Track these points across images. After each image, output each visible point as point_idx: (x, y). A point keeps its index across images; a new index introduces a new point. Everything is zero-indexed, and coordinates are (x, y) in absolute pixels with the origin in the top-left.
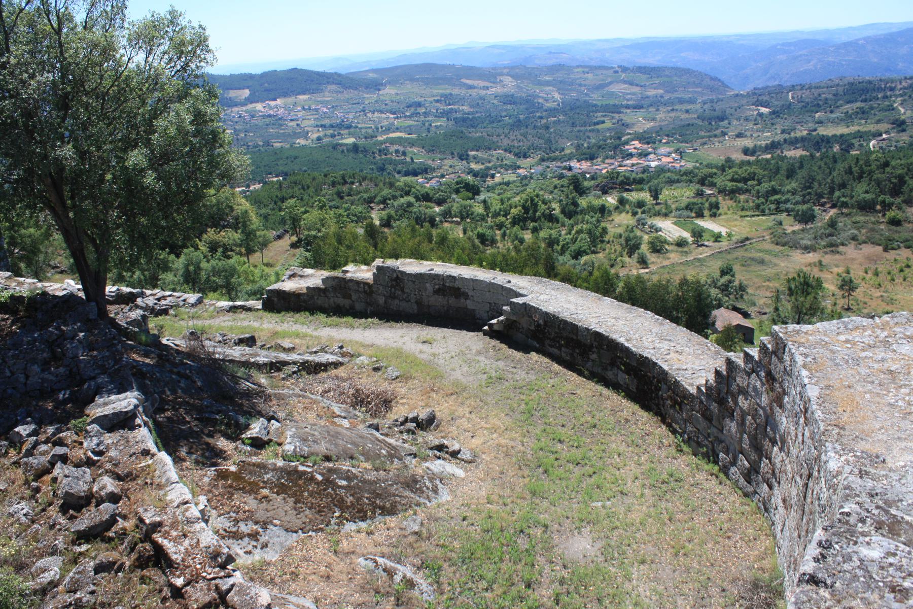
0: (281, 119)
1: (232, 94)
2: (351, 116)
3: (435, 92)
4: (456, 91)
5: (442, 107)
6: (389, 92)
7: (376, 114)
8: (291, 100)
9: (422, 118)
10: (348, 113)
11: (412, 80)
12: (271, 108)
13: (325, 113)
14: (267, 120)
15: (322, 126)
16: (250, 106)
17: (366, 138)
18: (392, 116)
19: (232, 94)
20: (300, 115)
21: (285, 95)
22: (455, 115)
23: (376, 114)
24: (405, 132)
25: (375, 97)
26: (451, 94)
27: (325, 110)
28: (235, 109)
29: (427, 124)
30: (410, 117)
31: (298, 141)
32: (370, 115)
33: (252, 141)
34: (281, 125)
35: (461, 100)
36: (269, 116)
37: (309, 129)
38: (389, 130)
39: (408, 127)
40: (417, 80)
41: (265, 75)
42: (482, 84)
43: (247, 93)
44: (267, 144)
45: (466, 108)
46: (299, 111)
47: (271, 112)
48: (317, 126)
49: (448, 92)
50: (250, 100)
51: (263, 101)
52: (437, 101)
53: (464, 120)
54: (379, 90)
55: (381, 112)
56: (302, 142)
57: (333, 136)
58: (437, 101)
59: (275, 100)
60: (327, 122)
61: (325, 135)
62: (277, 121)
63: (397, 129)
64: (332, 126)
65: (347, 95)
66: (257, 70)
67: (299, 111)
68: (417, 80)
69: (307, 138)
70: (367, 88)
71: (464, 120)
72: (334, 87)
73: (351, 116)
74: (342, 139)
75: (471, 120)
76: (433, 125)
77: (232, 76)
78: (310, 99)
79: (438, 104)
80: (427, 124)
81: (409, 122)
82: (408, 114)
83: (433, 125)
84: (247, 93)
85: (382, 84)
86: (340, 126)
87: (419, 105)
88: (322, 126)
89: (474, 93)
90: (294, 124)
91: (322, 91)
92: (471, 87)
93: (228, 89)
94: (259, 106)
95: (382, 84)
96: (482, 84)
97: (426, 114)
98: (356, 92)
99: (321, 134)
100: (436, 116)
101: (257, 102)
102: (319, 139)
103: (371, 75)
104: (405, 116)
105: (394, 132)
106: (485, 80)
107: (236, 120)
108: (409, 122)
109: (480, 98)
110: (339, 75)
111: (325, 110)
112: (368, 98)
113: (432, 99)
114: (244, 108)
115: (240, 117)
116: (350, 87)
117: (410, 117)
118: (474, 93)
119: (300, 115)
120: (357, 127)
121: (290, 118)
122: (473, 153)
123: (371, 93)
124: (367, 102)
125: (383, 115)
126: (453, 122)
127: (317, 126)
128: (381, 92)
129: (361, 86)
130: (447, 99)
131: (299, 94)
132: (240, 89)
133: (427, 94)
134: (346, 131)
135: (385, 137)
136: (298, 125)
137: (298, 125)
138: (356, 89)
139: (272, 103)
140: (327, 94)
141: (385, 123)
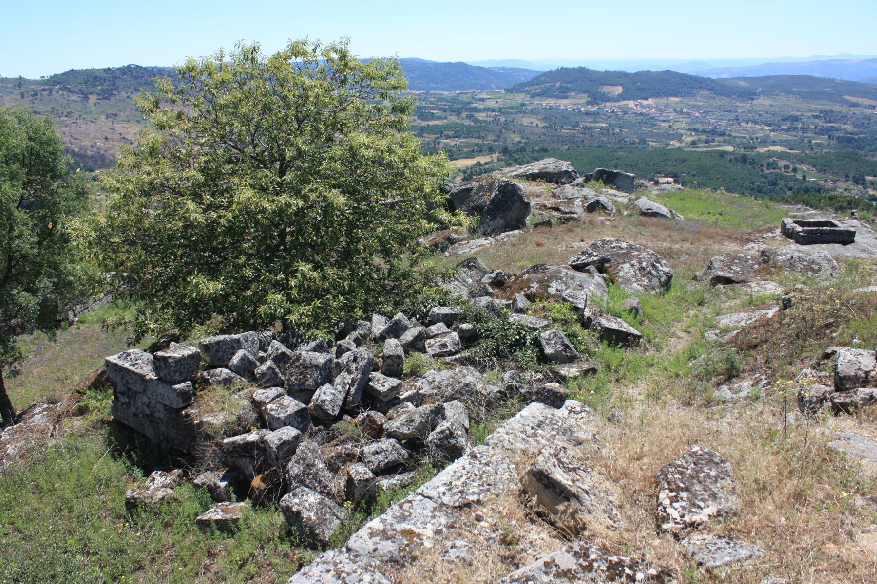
0: (653, 118)
1: (606, 89)
2: (724, 123)
3: (813, 106)
4: (837, 108)
5: (821, 123)
6: (763, 102)
7: (750, 124)
8: (662, 101)
9: (800, 133)
10: (720, 120)
11: (788, 92)
12: (642, 106)
13: (697, 117)
14: (640, 118)
15: (695, 130)
16: (623, 103)
17: (745, 148)
18: (767, 128)
19: (606, 89)
20: (672, 116)
21: (657, 95)
22: (837, 134)
23: (750, 124)
24: (785, 146)
25: (748, 106)
26: (832, 111)
27: (697, 114)
28: (608, 104)
29: (806, 140)
30: (787, 131)
31: (672, 142)
32: (743, 124)
33: (627, 137)
34: (654, 125)
35: (844, 118)
36: (642, 114)
37: (682, 132)
38: (764, 142)
39: (786, 141)
40: (794, 93)
41: (638, 74)
42: (868, 102)
43: (619, 90)
44: (644, 142)
45: (849, 127)
46: (671, 113)
47: (643, 111)
48: (690, 129)
49: (828, 108)
50: (622, 97)
51: (634, 98)
52: (816, 117)
53: (847, 140)
54: (753, 99)
55: (756, 123)
56: (677, 144)
57: (707, 142)
58: (816, 117)
59: (647, 99)
60: (698, 126)
61: (699, 140)
62: (650, 121)
63: (774, 143)
64: (704, 132)
65: (719, 101)
66: (631, 69)
67: (671, 113)
68: (794, 93)
69: (681, 141)
70: (740, 96)
71: (849, 140)
72: (705, 92)
73: (724, 123)
74: (718, 146)
75: (856, 141)
76: (813, 142)
77: (606, 72)
78: (681, 102)
79: (816, 121)
80: (806, 140)
81: (785, 137)
82: (784, 127)
83: (813, 142)
84: (619, 90)
85: (755, 94)
86: (714, 132)
87: (796, 119)
88: (695, 130)
89: (858, 111)
90: (666, 125)
91: (694, 95)
92: (854, 105)
93: (602, 84)
94: (631, 104)
95: (755, 94)
96: (868, 102)
97: (804, 130)
98: (728, 100)
99: (695, 138)
100: (815, 133)
101: (630, 99)
102: (693, 143)
103: (742, 83)
104: (782, 130)
105: (774, 145)
106: (870, 99)
107: (609, 115)
108: (785, 137)
109: (865, 118)
110: (712, 81)
111: (697, 114)
112: (741, 107)
113: (810, 114)
114: (617, 104)
115: (613, 112)
116: (722, 94)
117: (787, 131)
118: (858, 111)
119: (672, 116)
120: (730, 135)
121: (661, 118)
122: (869, 178)
123: (743, 102)
124: (739, 111)
125: (758, 126)
126: (835, 142)
127: (690, 129)
128: (754, 102)
129: (733, 94)
130: (827, 115)
131: (671, 96)
132: (613, 85)
133: (805, 109)
134: (721, 139)
135: (767, 149)
136: (670, 126)
137: (670, 126)
138: (729, 96)
139: (644, 102)
140: (698, 98)
141: (760, 135)
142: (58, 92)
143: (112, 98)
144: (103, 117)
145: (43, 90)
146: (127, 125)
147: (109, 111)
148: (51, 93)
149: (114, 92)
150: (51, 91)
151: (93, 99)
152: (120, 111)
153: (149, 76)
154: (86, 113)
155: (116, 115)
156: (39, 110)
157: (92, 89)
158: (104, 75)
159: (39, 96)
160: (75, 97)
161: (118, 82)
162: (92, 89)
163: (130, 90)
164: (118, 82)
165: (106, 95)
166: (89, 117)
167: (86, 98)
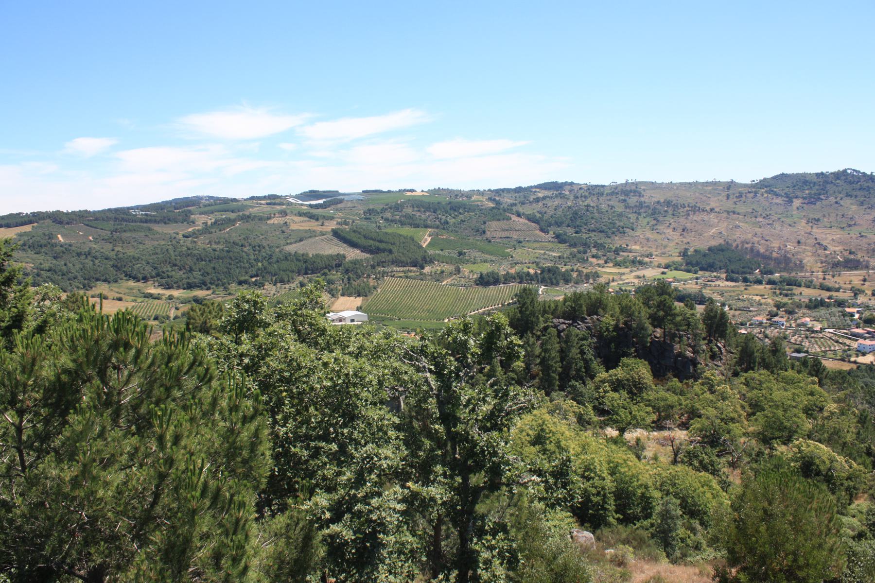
142: (762, 195)
143: (818, 203)
144: (804, 221)
145: (749, 192)
146: (828, 231)
147: (811, 216)
148: (755, 196)
149: (822, 197)
150: (756, 193)
151: (797, 203)
152: (824, 216)
153: (867, 181)
154: (787, 216)
155: (818, 220)
156: (737, 210)
157: (798, 193)
158: (815, 179)
159: (743, 199)
160: (779, 200)
161: (828, 186)
162: (798, 193)
163: (841, 195)
164: (828, 186)
165: (812, 200)
166: (788, 220)
167: (790, 201)
